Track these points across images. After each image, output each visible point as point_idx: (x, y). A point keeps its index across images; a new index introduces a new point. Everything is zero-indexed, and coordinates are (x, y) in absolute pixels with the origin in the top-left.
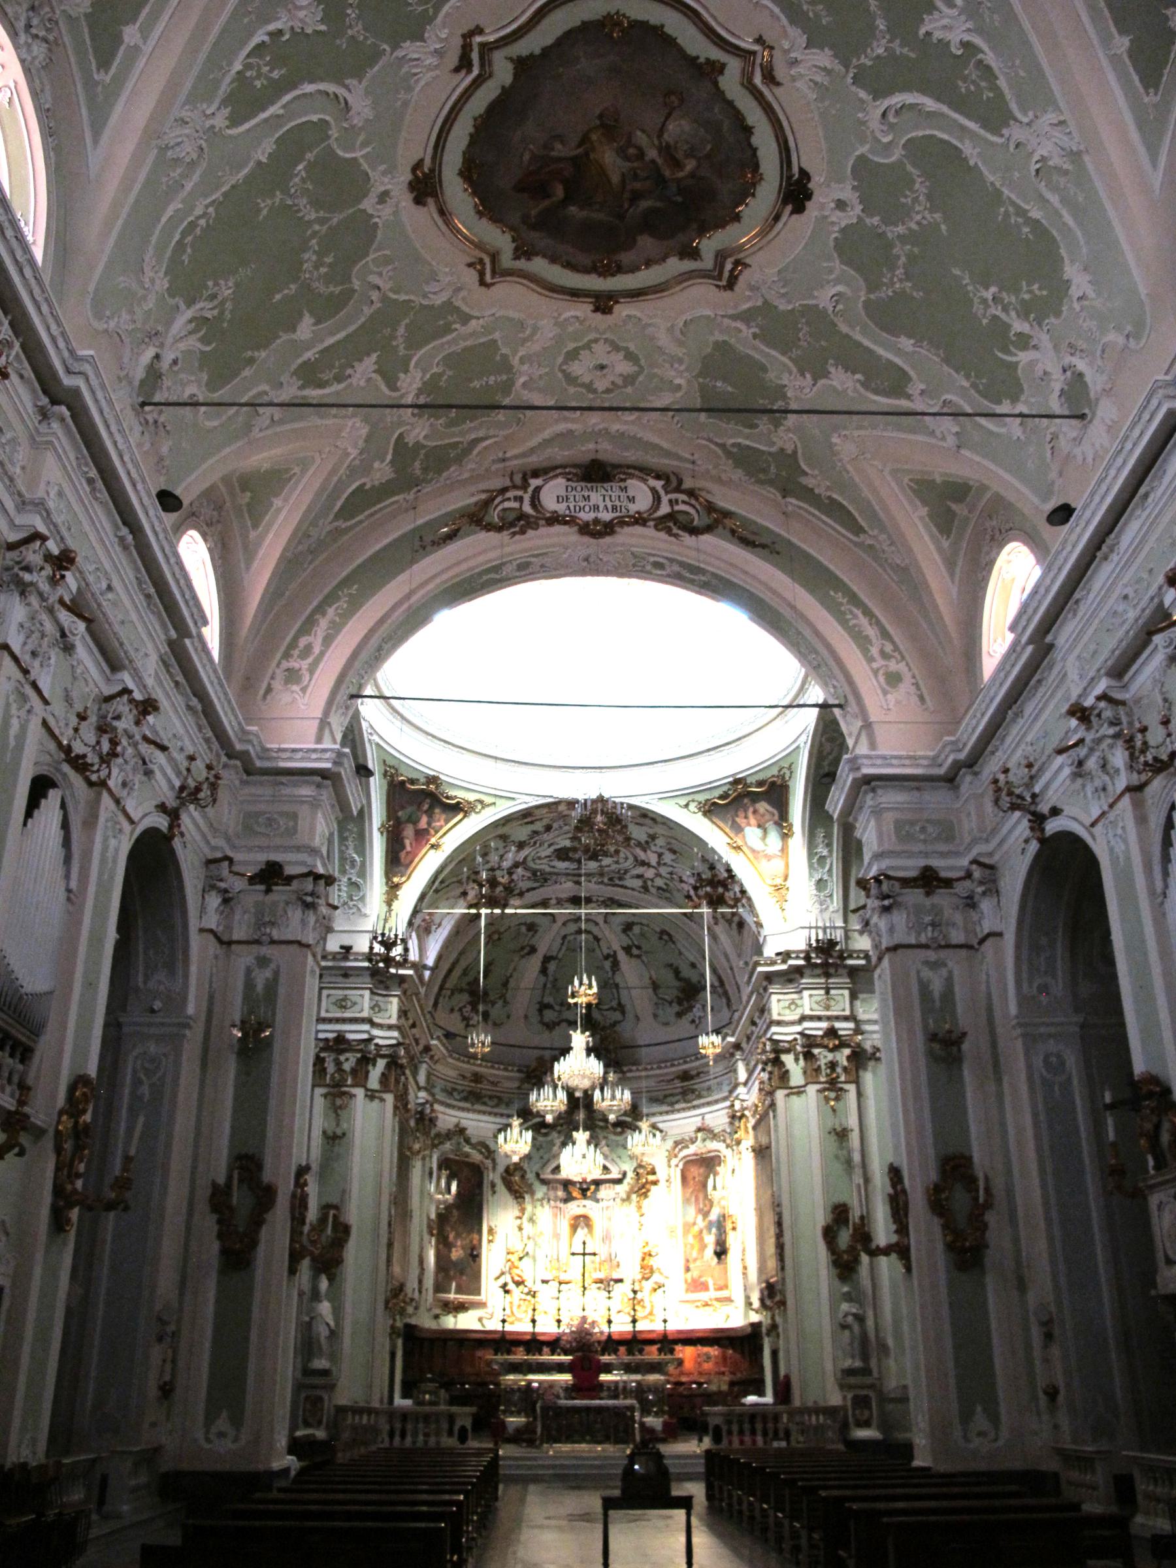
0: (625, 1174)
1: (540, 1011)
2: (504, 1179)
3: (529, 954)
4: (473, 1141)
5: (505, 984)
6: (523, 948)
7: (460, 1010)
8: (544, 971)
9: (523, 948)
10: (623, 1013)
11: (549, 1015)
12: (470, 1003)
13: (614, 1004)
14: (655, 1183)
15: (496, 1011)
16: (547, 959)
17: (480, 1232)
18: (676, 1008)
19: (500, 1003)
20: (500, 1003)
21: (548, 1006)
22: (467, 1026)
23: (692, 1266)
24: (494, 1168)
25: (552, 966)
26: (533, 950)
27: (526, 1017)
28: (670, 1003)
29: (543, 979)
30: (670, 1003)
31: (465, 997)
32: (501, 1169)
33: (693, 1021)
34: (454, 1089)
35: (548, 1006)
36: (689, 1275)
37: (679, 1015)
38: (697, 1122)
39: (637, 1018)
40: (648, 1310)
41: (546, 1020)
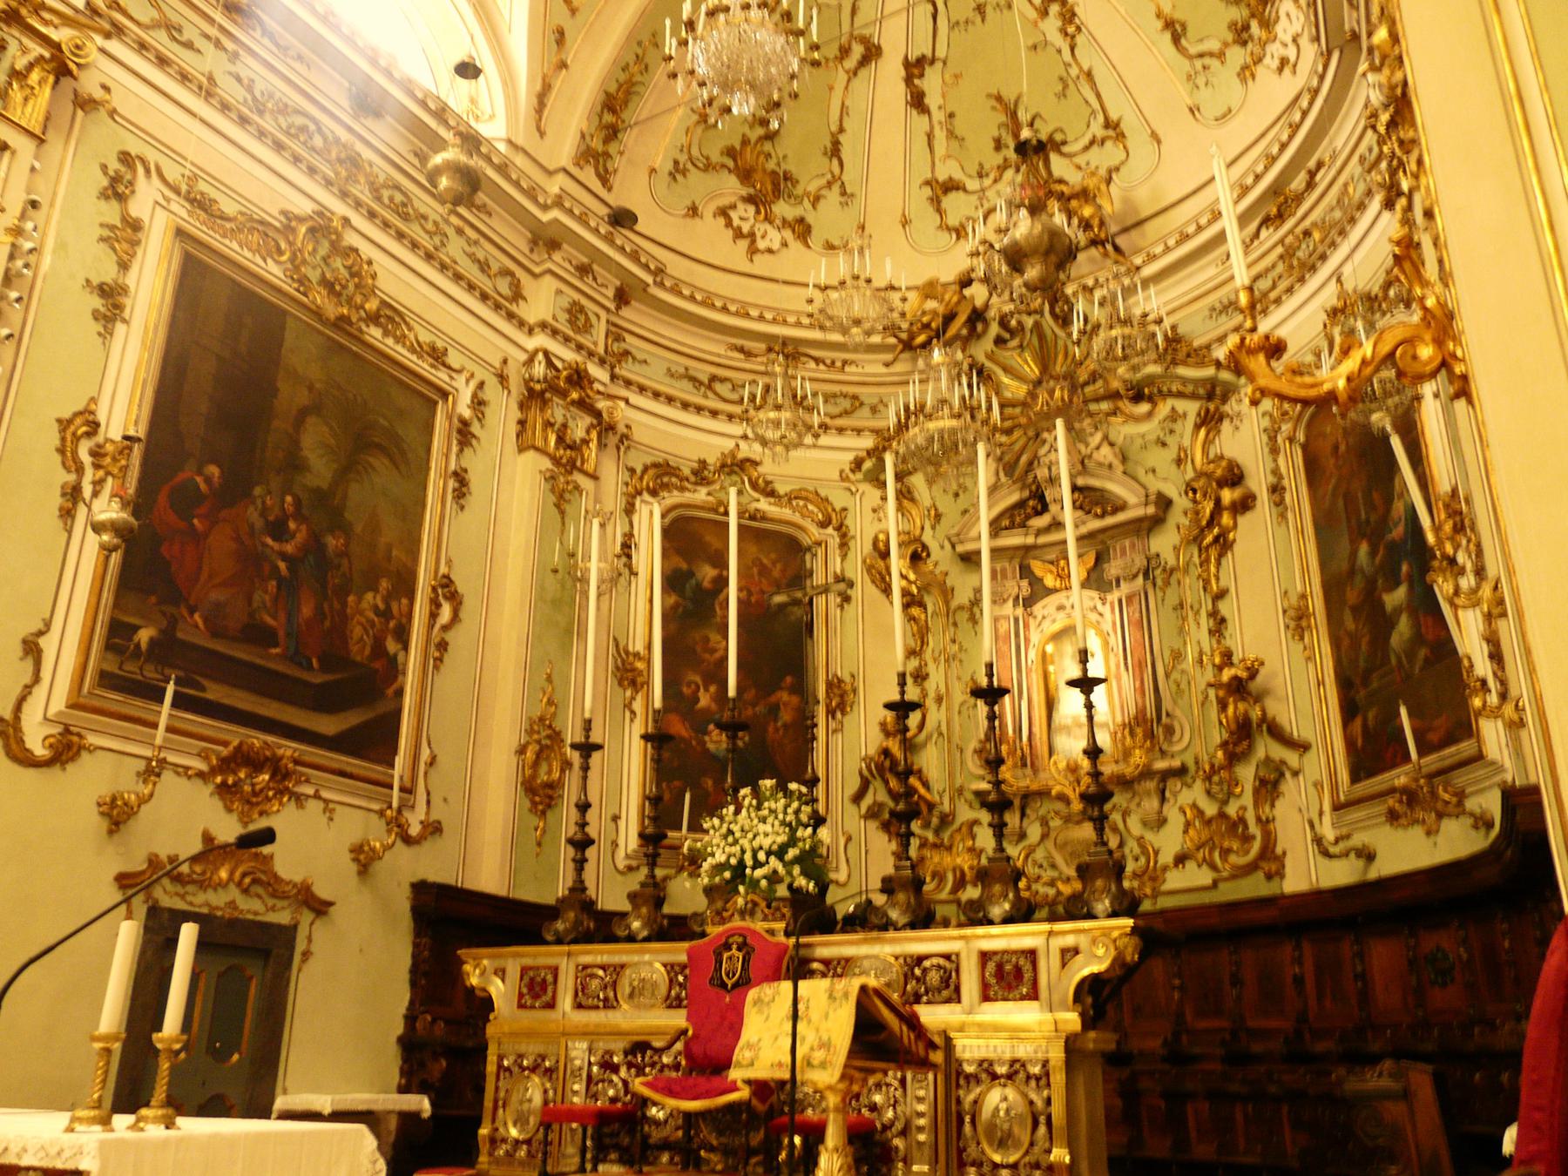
0: (1165, 503)
1: (936, 202)
2: (869, 569)
3: (865, 61)
4: (782, 489)
5: (835, 151)
6: (845, 52)
7: (723, 212)
8: (918, 101)
9: (845, 52)
10: (1121, 136)
11: (957, 207)
12: (750, 200)
13: (1097, 129)
14: (1245, 505)
15: (828, 218)
16: (915, 68)
17: (802, 688)
18: (1237, 56)
19: (833, 196)
20: (833, 196)
21: (951, 186)
22: (753, 251)
23: (1361, 695)
24: (844, 546)
25: (931, 83)
26: (872, 53)
27: (905, 222)
28: (1220, 56)
29: (921, 122)
30: (1220, 56)
31: (731, 187)
32: (861, 547)
33: (1284, 62)
34: (713, 378)
35: (951, 186)
36: (1357, 724)
37: (1246, 73)
38: (1329, 296)
39: (1155, 137)
40: (1256, 846)
41: (953, 221)
